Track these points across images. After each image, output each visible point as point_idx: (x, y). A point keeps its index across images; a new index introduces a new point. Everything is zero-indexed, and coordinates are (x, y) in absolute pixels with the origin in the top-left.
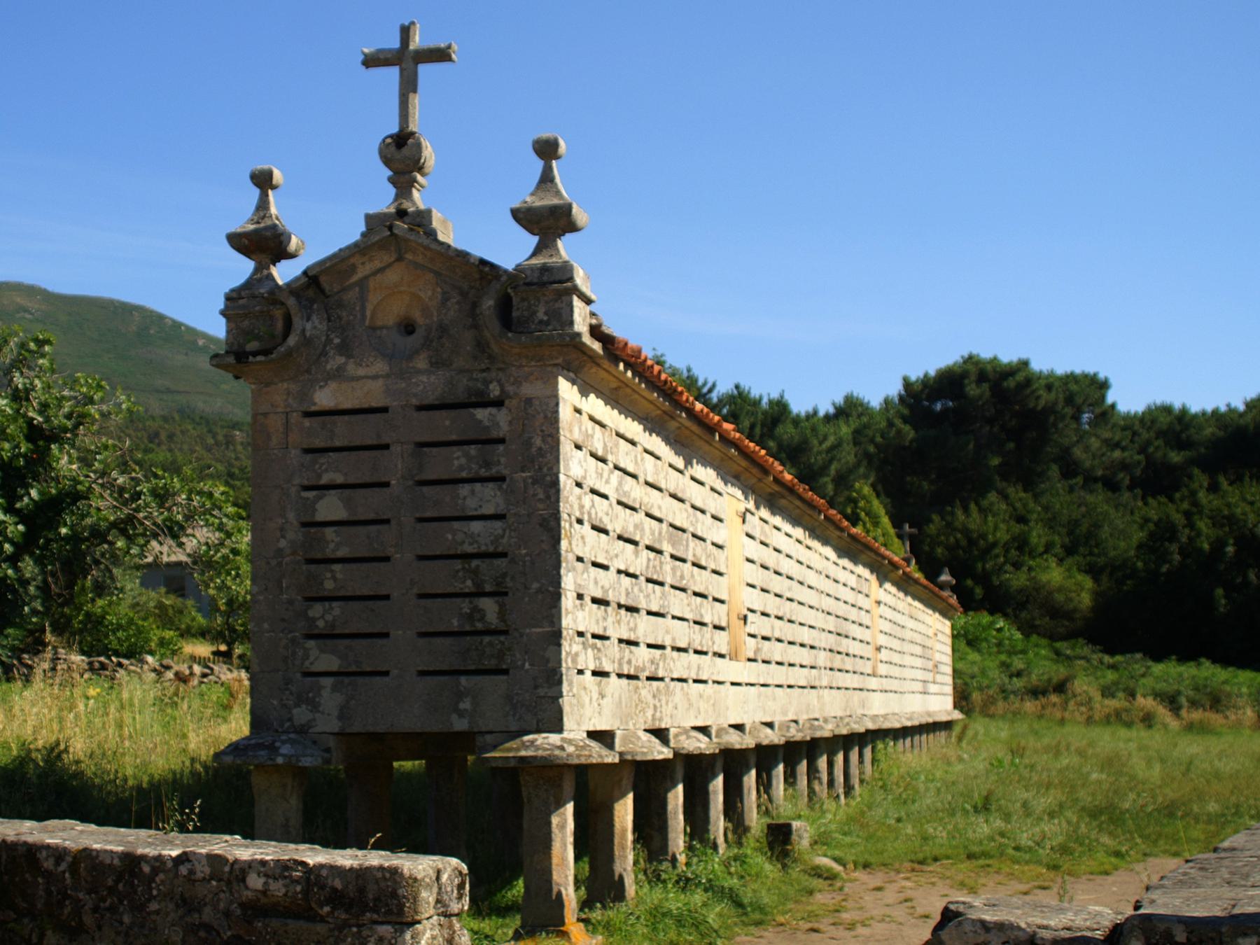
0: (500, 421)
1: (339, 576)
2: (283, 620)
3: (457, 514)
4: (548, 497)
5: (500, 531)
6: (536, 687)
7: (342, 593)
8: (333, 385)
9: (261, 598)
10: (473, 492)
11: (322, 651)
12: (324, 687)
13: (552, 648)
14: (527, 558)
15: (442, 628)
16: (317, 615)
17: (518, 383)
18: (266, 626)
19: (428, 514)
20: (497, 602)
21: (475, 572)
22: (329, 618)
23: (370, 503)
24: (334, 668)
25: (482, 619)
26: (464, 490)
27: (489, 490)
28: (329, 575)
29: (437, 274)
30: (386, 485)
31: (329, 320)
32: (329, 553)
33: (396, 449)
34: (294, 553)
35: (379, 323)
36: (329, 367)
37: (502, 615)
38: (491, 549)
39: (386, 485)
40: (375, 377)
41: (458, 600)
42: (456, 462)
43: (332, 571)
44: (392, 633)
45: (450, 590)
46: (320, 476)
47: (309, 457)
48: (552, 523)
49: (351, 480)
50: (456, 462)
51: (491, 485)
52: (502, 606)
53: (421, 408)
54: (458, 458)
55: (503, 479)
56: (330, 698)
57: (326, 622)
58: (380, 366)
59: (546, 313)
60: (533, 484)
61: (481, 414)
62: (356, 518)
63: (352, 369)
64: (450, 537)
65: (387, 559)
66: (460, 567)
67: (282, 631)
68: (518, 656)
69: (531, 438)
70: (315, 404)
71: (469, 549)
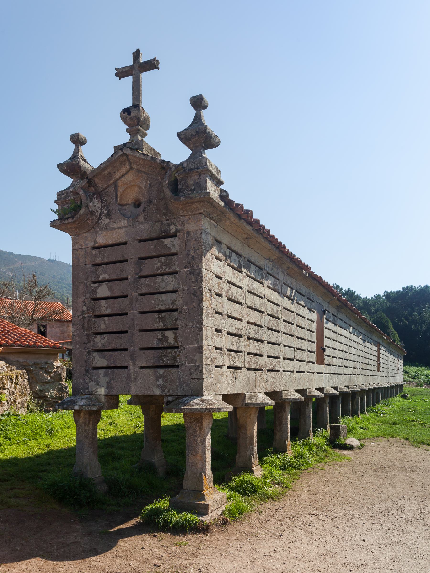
0: (173, 244)
1: (107, 322)
2: (85, 343)
3: (156, 291)
4: (197, 281)
5: (175, 298)
7: (108, 330)
8: (104, 233)
9: (76, 333)
10: (163, 279)
13: (198, 355)
15: (150, 346)
17: (183, 224)
18: (78, 346)
20: (174, 333)
22: (103, 342)
24: (105, 365)
25: (167, 341)
26: (159, 279)
27: (169, 279)
28: (103, 322)
30: (126, 279)
31: (102, 202)
32: (103, 312)
35: (124, 203)
37: (176, 339)
39: (126, 279)
40: (121, 228)
41: (157, 332)
42: (155, 266)
44: (128, 348)
45: (153, 328)
47: (95, 268)
48: (198, 293)
49: (113, 277)
50: (155, 266)
51: (171, 276)
52: (176, 334)
53: (141, 241)
55: (176, 273)
58: (124, 223)
60: (190, 274)
61: (167, 241)
62: (114, 295)
63: (111, 225)
64: (153, 302)
66: (157, 316)
67: (84, 349)
68: (183, 359)
69: (189, 251)
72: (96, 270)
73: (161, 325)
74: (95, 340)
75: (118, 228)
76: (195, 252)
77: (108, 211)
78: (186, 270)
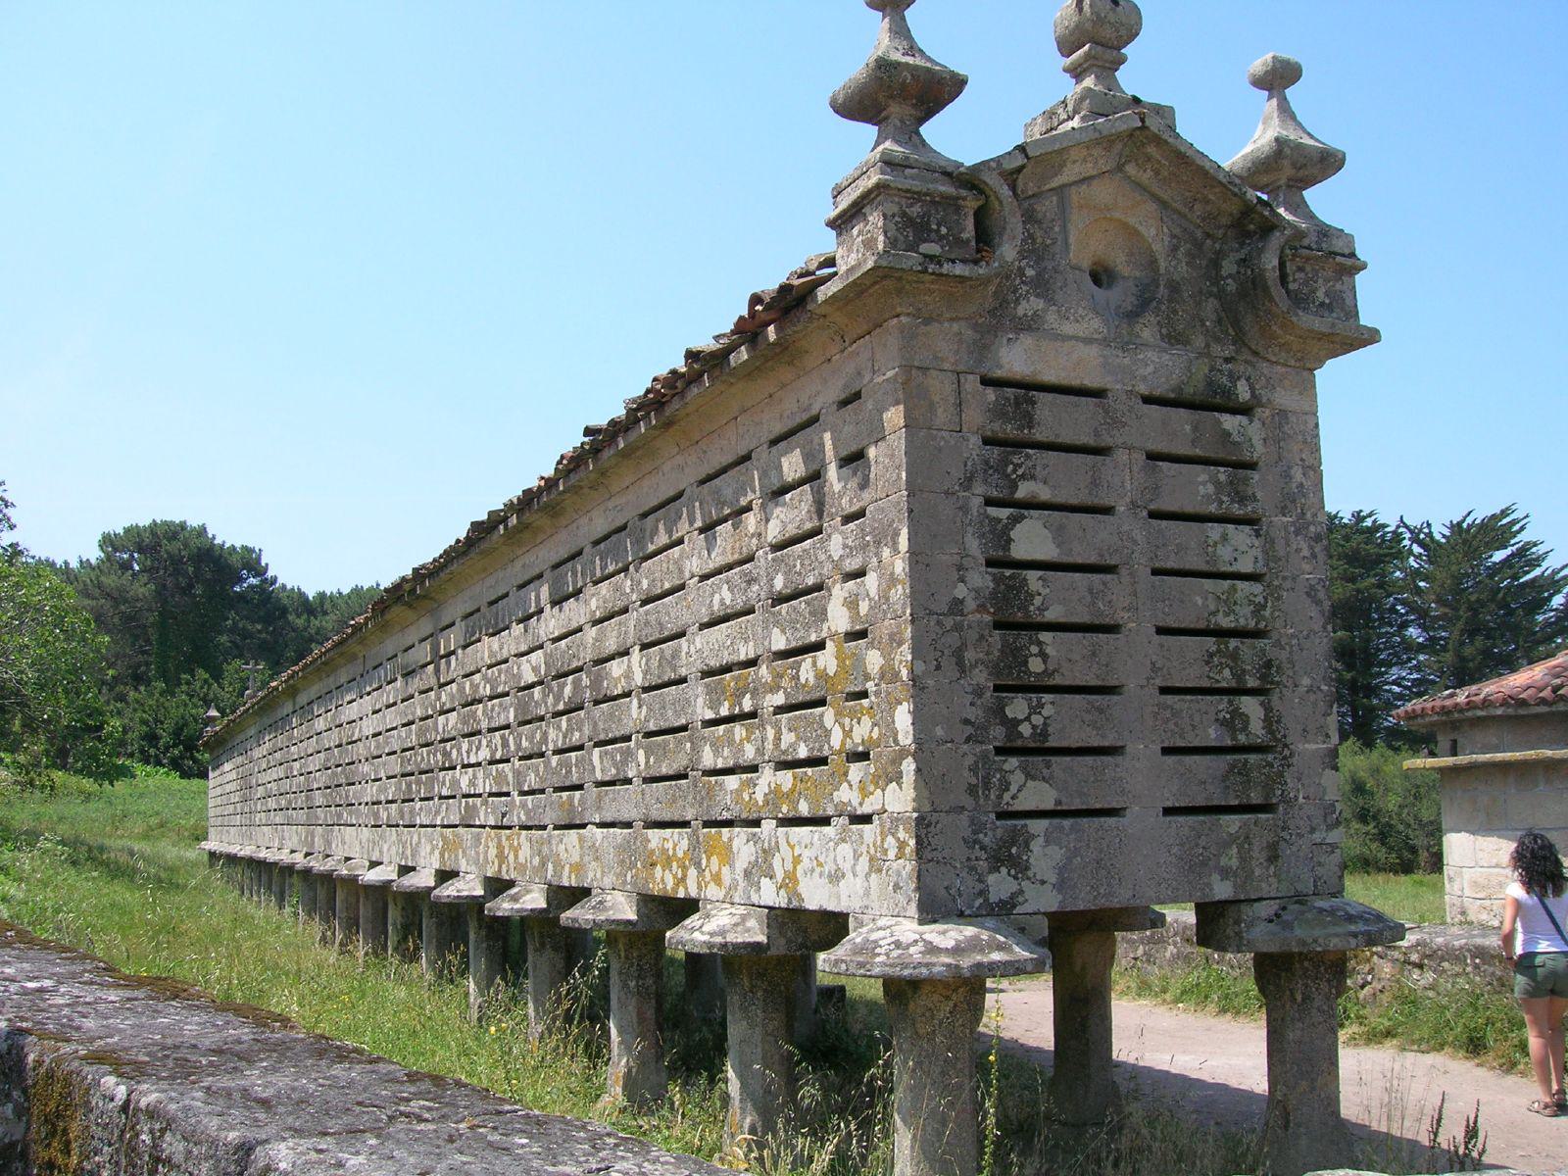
1: (1049, 650)
6: (1313, 830)
8: (1027, 340)
11: (1029, 776)
12: (1033, 837)
14: (1294, 641)
16: (1021, 717)
19: (1170, 564)
20: (1262, 704)
21: (1234, 656)
23: (1091, 539)
24: (1049, 805)
25: (1245, 728)
26: (1215, 531)
27: (1241, 536)
28: (1034, 649)
29: (1164, 204)
30: (1107, 511)
33: (1121, 456)
34: (981, 608)
36: (1020, 311)
37: (1270, 721)
38: (1252, 624)
39: (1107, 511)
43: (1040, 643)
46: (1014, 487)
52: (1268, 708)
53: (1148, 400)
54: (1204, 483)
56: (1044, 855)
57: (1034, 727)
59: (1327, 294)
61: (1229, 422)
63: (1051, 318)
65: (1111, 629)
68: (1290, 785)
70: (1000, 367)
71: (1226, 622)
72: (1005, 462)
73: (1226, 678)
74: (1009, 712)
75: (1076, 338)
76: (1304, 475)
77: (1039, 274)
78: (1285, 519)
